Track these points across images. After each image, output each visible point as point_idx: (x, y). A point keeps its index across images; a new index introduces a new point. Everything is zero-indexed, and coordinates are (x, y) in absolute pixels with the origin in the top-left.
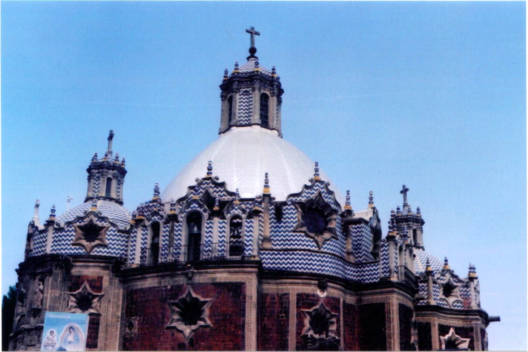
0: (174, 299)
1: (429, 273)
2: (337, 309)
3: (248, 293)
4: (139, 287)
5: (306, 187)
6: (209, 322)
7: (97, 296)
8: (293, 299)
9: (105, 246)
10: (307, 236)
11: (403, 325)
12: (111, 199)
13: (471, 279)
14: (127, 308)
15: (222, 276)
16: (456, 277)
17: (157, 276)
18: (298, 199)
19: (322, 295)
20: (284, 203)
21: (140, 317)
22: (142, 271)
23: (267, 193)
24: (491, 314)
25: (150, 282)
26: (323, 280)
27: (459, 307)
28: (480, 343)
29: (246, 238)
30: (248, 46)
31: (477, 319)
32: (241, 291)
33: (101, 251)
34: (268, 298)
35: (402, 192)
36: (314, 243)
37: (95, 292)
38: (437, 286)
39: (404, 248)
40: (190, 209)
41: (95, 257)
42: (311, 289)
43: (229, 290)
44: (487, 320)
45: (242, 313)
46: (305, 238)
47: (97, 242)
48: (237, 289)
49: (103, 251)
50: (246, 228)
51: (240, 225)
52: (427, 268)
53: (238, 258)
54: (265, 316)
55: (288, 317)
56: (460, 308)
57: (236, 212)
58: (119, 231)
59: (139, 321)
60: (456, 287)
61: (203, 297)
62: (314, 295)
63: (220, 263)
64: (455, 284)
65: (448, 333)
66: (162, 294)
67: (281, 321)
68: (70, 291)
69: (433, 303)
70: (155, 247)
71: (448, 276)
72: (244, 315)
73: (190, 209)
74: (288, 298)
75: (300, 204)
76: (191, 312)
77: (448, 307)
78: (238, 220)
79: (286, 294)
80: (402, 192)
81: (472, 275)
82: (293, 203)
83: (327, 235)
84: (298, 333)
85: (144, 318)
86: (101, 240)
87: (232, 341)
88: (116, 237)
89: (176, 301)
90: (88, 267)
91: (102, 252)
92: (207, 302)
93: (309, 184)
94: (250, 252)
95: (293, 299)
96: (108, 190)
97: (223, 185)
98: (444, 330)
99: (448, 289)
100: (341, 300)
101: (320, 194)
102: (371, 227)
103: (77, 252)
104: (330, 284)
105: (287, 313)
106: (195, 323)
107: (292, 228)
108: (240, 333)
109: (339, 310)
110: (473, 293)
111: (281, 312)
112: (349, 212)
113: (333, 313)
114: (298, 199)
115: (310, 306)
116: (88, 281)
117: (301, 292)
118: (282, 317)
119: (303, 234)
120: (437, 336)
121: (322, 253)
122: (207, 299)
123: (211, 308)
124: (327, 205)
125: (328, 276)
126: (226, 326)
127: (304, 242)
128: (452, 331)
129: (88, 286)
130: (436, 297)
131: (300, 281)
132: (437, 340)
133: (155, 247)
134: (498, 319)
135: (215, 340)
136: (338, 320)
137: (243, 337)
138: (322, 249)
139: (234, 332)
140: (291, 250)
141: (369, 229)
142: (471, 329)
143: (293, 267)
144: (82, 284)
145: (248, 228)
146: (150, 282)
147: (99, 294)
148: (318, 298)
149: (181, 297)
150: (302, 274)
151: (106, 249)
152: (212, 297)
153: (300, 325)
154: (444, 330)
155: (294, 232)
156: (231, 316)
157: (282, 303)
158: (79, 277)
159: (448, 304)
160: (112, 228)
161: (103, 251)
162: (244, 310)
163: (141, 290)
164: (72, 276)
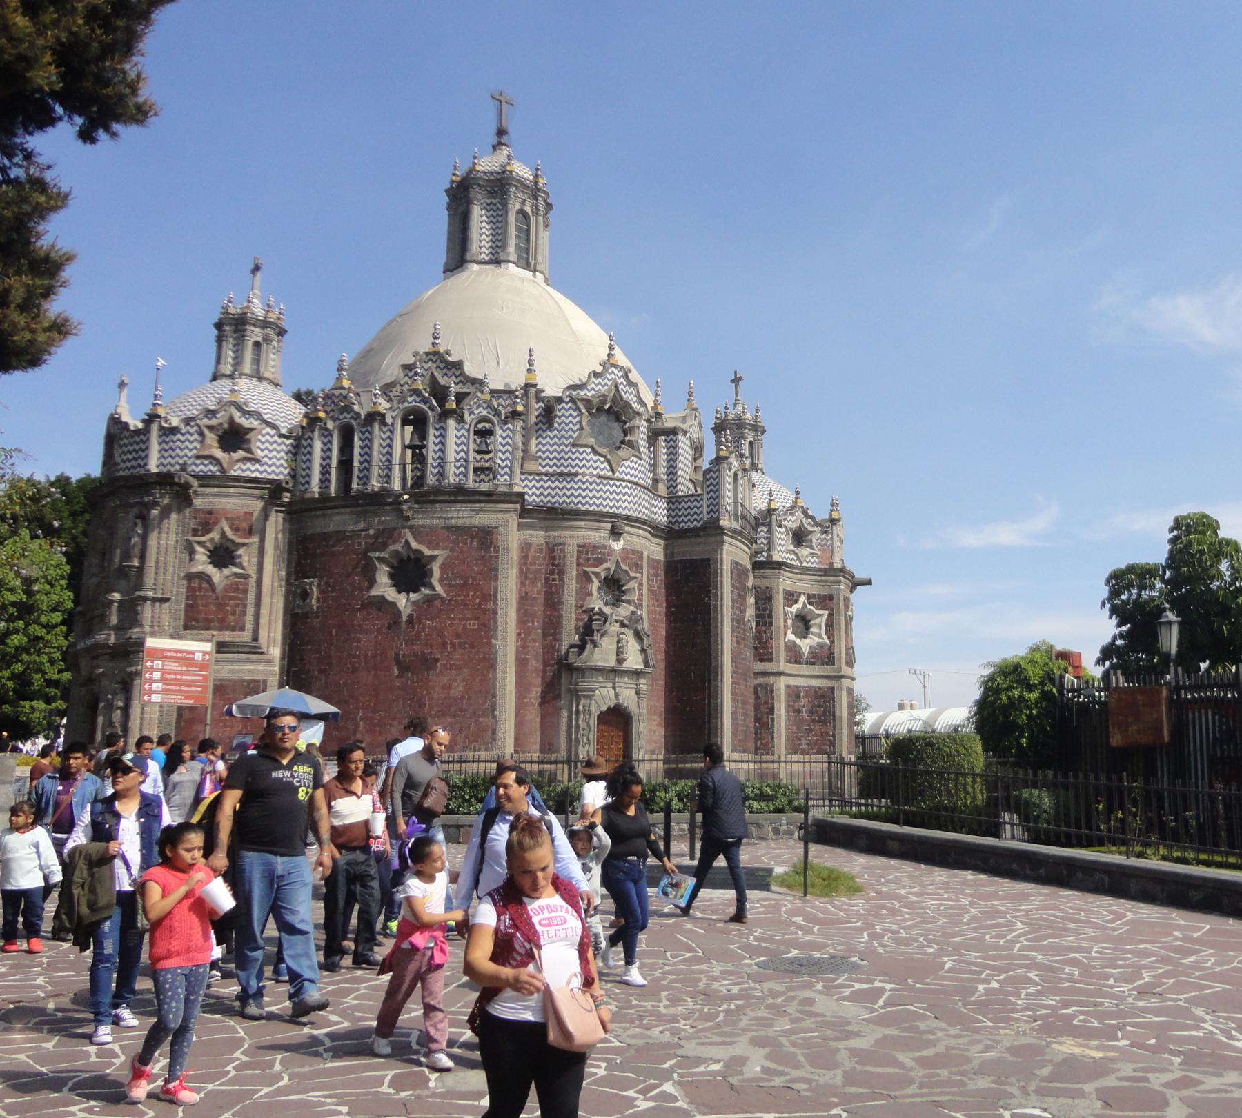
0: (381, 551)
1: (770, 511)
2: (638, 567)
3: (501, 543)
4: (319, 530)
5: (596, 375)
6: (439, 589)
7: (244, 545)
9: (257, 461)
10: (595, 452)
11: (736, 592)
12: (260, 379)
13: (833, 521)
14: (298, 563)
15: (463, 515)
16: (812, 517)
17: (351, 513)
18: (582, 393)
20: (559, 400)
21: (320, 578)
22: (325, 501)
23: (532, 382)
24: (859, 575)
25: (337, 521)
27: (812, 562)
28: (843, 618)
29: (500, 454)
31: (839, 582)
32: (491, 542)
33: (248, 469)
34: (532, 550)
35: (732, 381)
36: (605, 464)
37: (240, 537)
38: (783, 530)
39: (740, 475)
40: (406, 404)
41: (237, 479)
42: (598, 535)
43: (472, 538)
44: (855, 584)
45: (491, 572)
46: (592, 455)
47: (241, 454)
48: (485, 537)
49: (253, 468)
50: (500, 439)
51: (490, 433)
52: (769, 504)
53: (484, 487)
54: (526, 578)
55: (562, 580)
56: (815, 565)
57: (485, 413)
58: (281, 436)
59: (319, 585)
60: (811, 532)
61: (428, 548)
62: (604, 547)
63: (461, 494)
64: (810, 529)
65: (796, 602)
66: (360, 544)
67: (551, 586)
68: (194, 535)
69: (777, 557)
70: (346, 465)
71: (799, 513)
72: (496, 579)
73: (406, 404)
74: (563, 551)
75: (587, 402)
76: (410, 573)
77: (797, 563)
78: (487, 425)
79: (560, 544)
80: (732, 381)
81: (835, 515)
82: (573, 400)
84: (579, 606)
85: (327, 584)
86: (249, 451)
87: (477, 619)
88: (275, 446)
89: (383, 555)
90: (226, 495)
91: (252, 470)
92: (436, 556)
93: (599, 369)
94: (506, 477)
96: (257, 362)
97: (458, 365)
98: (791, 598)
99: (799, 537)
100: (645, 555)
101: (616, 387)
102: (692, 441)
103: (206, 469)
104: (628, 529)
105: (561, 573)
106: (416, 590)
107: (571, 440)
108: (490, 605)
109: (641, 568)
111: (552, 573)
113: (632, 574)
114: (582, 393)
115: (599, 562)
116: (227, 519)
117: (582, 541)
118: (554, 580)
119: (589, 450)
120: (781, 607)
121: (618, 480)
122: (436, 553)
124: (627, 405)
125: (628, 519)
126: (466, 596)
127: (591, 464)
128: (802, 599)
129: (227, 529)
130: (783, 549)
131: (583, 523)
132: (781, 614)
133: (346, 465)
134: (869, 583)
135: (449, 618)
136: (641, 584)
137: (495, 612)
138: (617, 474)
139: (480, 604)
140: (569, 474)
141: (688, 443)
142: (830, 598)
143: (572, 502)
144: (215, 524)
145: (504, 438)
146: (337, 521)
147: (246, 541)
148: (611, 552)
149: (392, 548)
150: (587, 513)
151: (257, 466)
152: (443, 549)
153: (584, 593)
154: (791, 598)
155: (574, 445)
156: (474, 579)
157: (554, 558)
158: (210, 512)
159: (798, 559)
160: (268, 429)
161: (253, 468)
162: (496, 570)
163: (325, 536)
164: (197, 511)
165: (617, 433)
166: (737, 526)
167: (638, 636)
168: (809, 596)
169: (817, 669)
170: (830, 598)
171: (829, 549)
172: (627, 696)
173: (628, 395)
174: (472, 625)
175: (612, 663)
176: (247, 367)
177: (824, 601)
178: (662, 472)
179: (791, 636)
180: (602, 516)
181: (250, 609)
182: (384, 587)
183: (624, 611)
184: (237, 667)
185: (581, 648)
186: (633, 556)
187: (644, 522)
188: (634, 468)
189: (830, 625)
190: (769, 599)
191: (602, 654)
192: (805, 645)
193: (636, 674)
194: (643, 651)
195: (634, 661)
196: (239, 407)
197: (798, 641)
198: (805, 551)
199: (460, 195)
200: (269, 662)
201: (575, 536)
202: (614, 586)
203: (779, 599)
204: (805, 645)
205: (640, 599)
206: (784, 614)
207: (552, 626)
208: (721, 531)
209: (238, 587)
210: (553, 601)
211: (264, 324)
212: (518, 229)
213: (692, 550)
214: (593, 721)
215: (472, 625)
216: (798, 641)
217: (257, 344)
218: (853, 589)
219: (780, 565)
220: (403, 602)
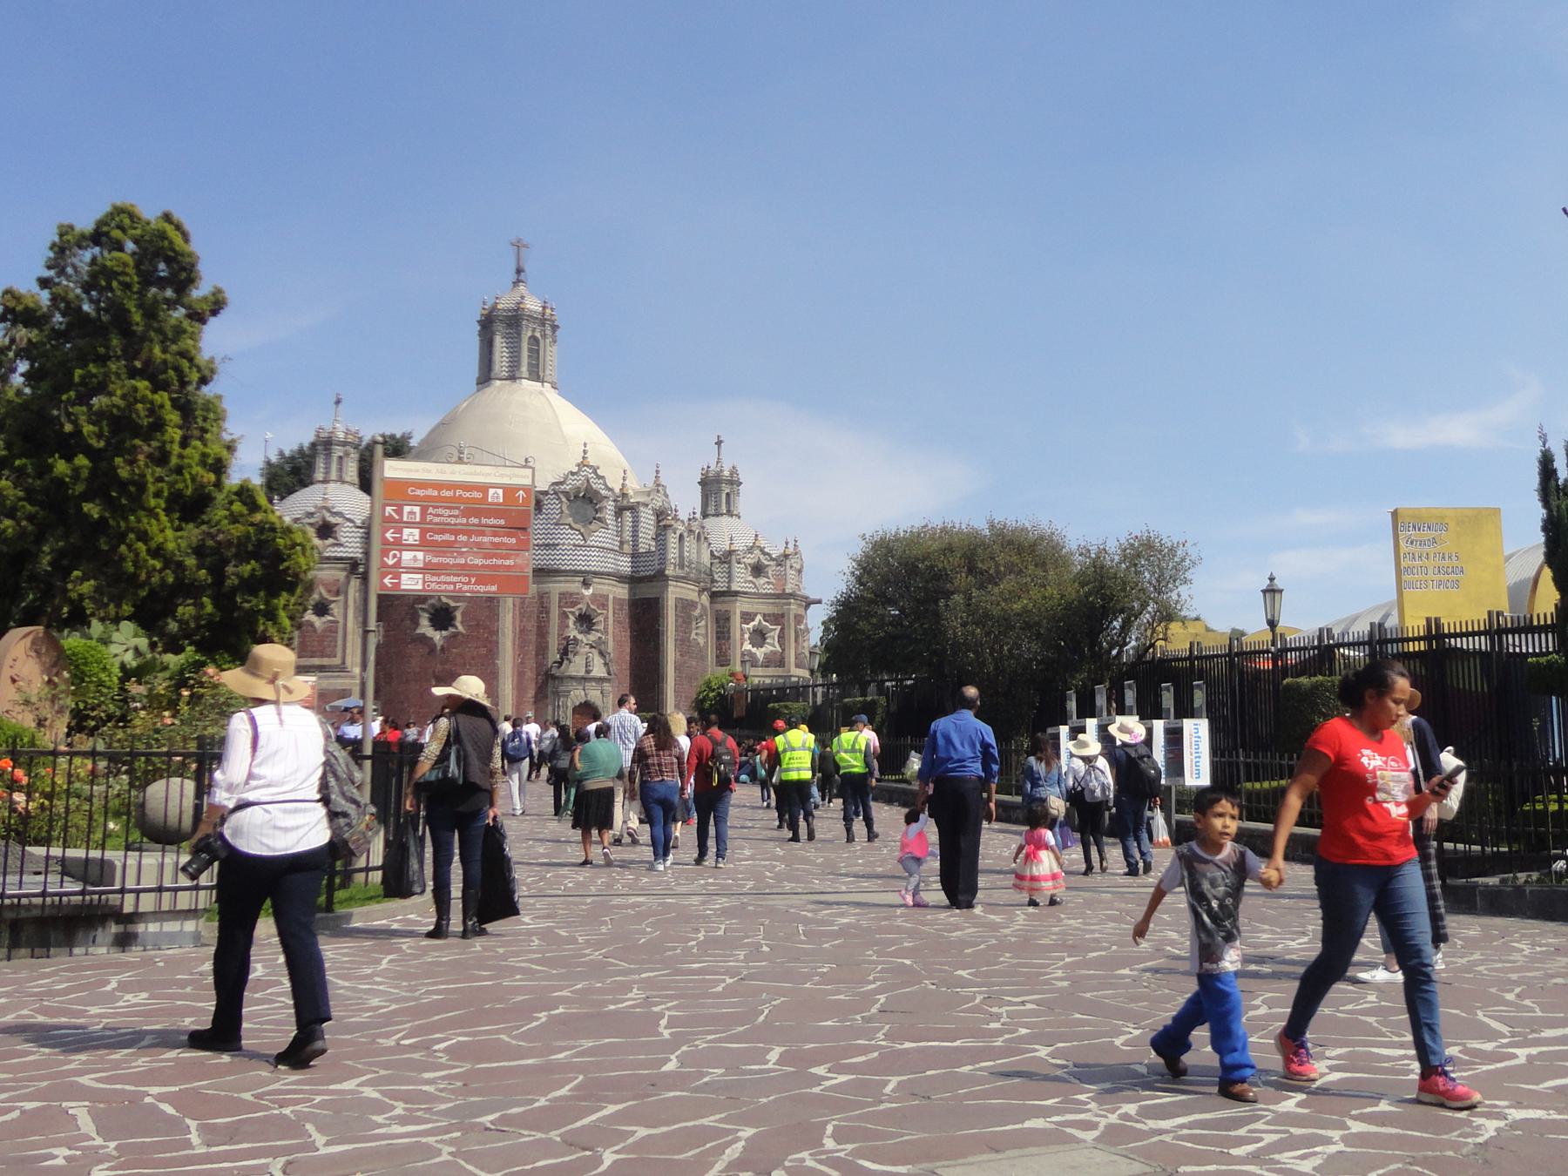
1: (731, 553)
2: (604, 606)
5: (573, 474)
6: (460, 628)
8: (555, 599)
12: (344, 482)
13: (786, 556)
19: (588, 592)
20: (546, 493)
24: (813, 597)
26: (587, 578)
27: (769, 589)
30: (513, 268)
41: (328, 558)
42: (574, 586)
47: (331, 541)
69: (735, 587)
71: (757, 552)
75: (566, 494)
83: (592, 527)
93: (575, 469)
95: (555, 599)
96: (340, 470)
98: (747, 617)
99: (758, 570)
105: (548, 613)
110: (791, 573)
112: (624, 495)
115: (574, 604)
123: (463, 614)
124: (597, 492)
125: (596, 573)
127: (569, 537)
128: (759, 617)
130: (741, 579)
136: (606, 619)
142: (783, 616)
153: (563, 626)
165: (591, 512)
166: (680, 573)
167: (602, 654)
168: (764, 616)
169: (771, 671)
170: (783, 616)
171: (782, 579)
172: (594, 695)
173: (597, 485)
174: (483, 651)
175: (582, 673)
176: (334, 475)
177: (777, 619)
178: (627, 536)
179: (747, 646)
180: (576, 573)
181: (340, 643)
182: (425, 628)
183: (593, 637)
184: (332, 681)
185: (561, 663)
186: (601, 601)
187: (608, 574)
188: (603, 536)
189: (781, 637)
190: (728, 619)
191: (576, 667)
192: (760, 653)
193: (601, 680)
194: (606, 664)
195: (598, 670)
196: (328, 509)
197: (754, 650)
198: (762, 580)
199: (488, 324)
200: (353, 677)
201: (556, 587)
202: (586, 621)
203: (736, 620)
204: (760, 653)
205: (606, 628)
206: (741, 633)
207: (542, 649)
208: (666, 578)
209: (332, 629)
210: (542, 632)
211: (344, 444)
212: (530, 350)
213: (647, 591)
214: (570, 712)
215: (483, 651)
216: (754, 650)
217: (340, 458)
218: (807, 607)
219: (736, 594)
220: (437, 636)
